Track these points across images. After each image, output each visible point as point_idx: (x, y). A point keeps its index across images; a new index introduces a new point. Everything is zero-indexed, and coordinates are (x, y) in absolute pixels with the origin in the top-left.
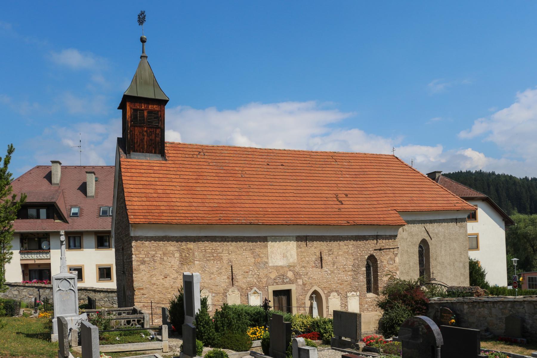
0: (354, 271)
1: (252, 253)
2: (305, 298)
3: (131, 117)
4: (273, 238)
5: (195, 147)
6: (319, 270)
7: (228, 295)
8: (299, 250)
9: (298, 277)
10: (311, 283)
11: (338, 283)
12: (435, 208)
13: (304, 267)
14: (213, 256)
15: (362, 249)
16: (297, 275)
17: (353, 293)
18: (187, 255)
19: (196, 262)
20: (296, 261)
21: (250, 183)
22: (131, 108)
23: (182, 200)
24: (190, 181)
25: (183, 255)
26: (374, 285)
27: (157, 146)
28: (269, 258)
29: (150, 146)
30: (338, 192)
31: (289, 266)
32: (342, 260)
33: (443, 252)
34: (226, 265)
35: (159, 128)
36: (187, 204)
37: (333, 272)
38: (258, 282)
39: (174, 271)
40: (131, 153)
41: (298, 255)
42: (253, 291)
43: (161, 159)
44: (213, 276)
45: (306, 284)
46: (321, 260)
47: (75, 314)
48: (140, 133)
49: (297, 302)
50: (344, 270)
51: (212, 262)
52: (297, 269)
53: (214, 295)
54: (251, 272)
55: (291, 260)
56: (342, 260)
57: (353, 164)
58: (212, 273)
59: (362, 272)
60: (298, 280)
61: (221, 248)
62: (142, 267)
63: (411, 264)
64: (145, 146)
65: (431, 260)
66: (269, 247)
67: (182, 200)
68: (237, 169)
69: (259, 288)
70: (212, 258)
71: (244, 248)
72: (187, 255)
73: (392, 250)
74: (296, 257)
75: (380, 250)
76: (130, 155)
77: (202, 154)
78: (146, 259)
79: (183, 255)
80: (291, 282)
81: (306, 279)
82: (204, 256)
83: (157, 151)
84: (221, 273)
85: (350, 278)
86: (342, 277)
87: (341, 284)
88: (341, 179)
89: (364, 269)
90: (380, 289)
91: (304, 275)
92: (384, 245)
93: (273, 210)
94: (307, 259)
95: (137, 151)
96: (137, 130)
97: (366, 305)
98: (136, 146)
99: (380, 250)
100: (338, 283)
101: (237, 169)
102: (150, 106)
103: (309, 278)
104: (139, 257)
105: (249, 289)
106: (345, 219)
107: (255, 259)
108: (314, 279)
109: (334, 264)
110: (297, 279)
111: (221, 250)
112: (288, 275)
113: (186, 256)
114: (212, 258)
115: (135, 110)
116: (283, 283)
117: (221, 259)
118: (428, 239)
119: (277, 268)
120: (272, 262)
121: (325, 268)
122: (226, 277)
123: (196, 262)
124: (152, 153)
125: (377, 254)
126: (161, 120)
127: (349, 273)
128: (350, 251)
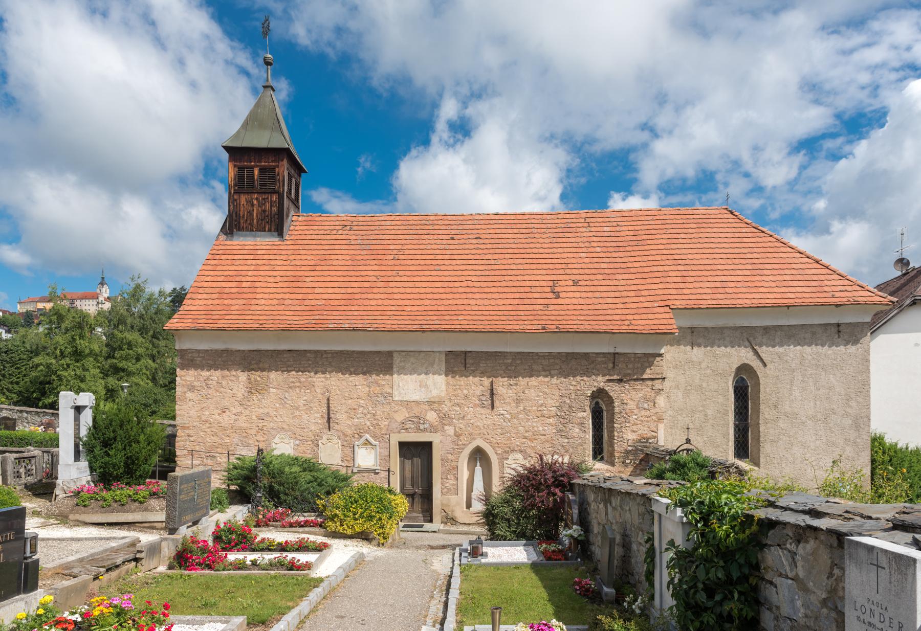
0: (561, 417)
2: (458, 458)
6: (489, 411)
7: (321, 445)
10: (471, 434)
11: (526, 438)
20: (443, 394)
28: (395, 387)
31: (430, 403)
33: (797, 393)
34: (320, 397)
35: (275, 192)
37: (514, 416)
38: (373, 425)
39: (237, 403)
42: (363, 440)
44: (298, 413)
50: (539, 414)
52: (445, 408)
53: (297, 442)
55: (435, 393)
60: (446, 428)
62: (189, 395)
63: (709, 412)
69: (375, 437)
70: (298, 384)
71: (352, 370)
72: (259, 379)
73: (650, 383)
74: (444, 387)
78: (196, 384)
80: (433, 429)
81: (462, 426)
85: (550, 430)
86: (533, 427)
87: (530, 440)
90: (616, 455)
91: (458, 419)
94: (465, 391)
98: (242, 221)
99: (620, 381)
100: (526, 438)
103: (467, 425)
105: (356, 436)
107: (369, 387)
109: (518, 402)
110: (444, 424)
112: (427, 418)
113: (256, 380)
114: (298, 384)
116: (418, 430)
118: (755, 364)
119: (407, 404)
120: (400, 394)
122: (318, 415)
125: (614, 390)
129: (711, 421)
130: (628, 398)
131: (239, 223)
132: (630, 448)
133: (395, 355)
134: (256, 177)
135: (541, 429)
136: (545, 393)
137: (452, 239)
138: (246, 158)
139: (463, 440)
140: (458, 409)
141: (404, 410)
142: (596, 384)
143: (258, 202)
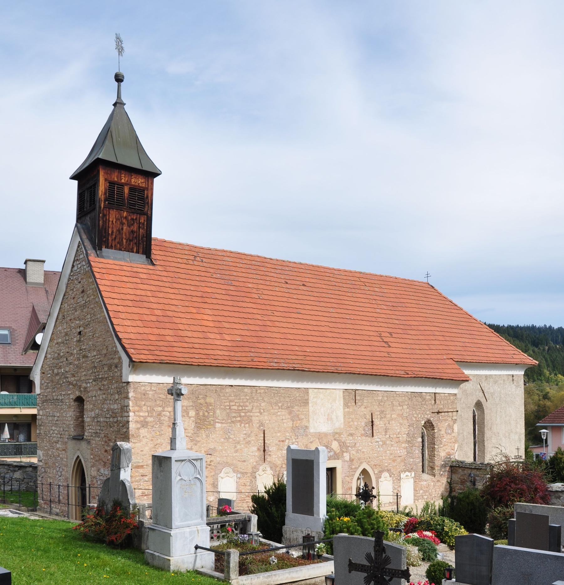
1: (290, 413)
3: (105, 194)
4: (316, 390)
5: (187, 248)
6: (369, 439)
7: (258, 476)
8: (347, 410)
9: (345, 450)
10: (359, 459)
12: (493, 359)
13: (351, 435)
14: (240, 416)
15: (418, 412)
16: (344, 446)
17: (407, 473)
18: (206, 414)
19: (218, 425)
21: (273, 308)
22: (106, 180)
23: (193, 328)
24: (195, 299)
25: (201, 414)
26: (429, 462)
27: (141, 242)
28: (311, 420)
29: (130, 241)
30: (381, 329)
32: (395, 427)
35: (144, 214)
36: (200, 335)
40: (104, 249)
41: (345, 416)
43: (146, 263)
44: (239, 447)
45: (353, 460)
46: (372, 425)
47: (199, 520)
48: (117, 219)
49: (343, 487)
51: (238, 424)
52: (344, 437)
53: (239, 475)
54: (287, 441)
55: (337, 425)
56: (395, 427)
57: (385, 291)
58: (238, 443)
59: (417, 444)
60: (345, 454)
61: (250, 403)
62: (143, 432)
63: (465, 434)
64: (124, 241)
65: (486, 429)
66: (310, 405)
67: (193, 328)
68: (250, 285)
70: (239, 419)
71: (280, 405)
72: (206, 414)
75: (438, 413)
76: (101, 253)
77: (198, 259)
78: (149, 419)
79: (201, 414)
81: (354, 452)
82: (228, 415)
83: (141, 250)
84: (248, 443)
85: (403, 452)
88: (378, 311)
89: (420, 440)
90: (436, 468)
91: (352, 447)
92: (442, 407)
93: (313, 350)
95: (111, 247)
96: (113, 215)
97: (421, 492)
99: (438, 413)
100: (390, 459)
101: (250, 285)
102: (133, 180)
103: (357, 452)
104: (140, 416)
106: (403, 368)
107: (293, 421)
108: (363, 452)
110: (343, 452)
111: (250, 408)
113: (204, 415)
114: (239, 419)
115: (112, 184)
117: (249, 421)
118: (483, 400)
121: (375, 437)
122: (255, 449)
123: (218, 425)
124: (133, 252)
125: (434, 419)
126: (148, 203)
127: (403, 445)
128: (405, 415)
129: (466, 440)
130: (441, 427)
131: (108, 239)
132: (443, 463)
133: (310, 391)
134: (126, 195)
135: (399, 452)
136: (401, 424)
137: (304, 285)
138: (116, 174)
139: (355, 464)
140: (351, 438)
141: (317, 440)
142: (426, 416)
143: (128, 221)
